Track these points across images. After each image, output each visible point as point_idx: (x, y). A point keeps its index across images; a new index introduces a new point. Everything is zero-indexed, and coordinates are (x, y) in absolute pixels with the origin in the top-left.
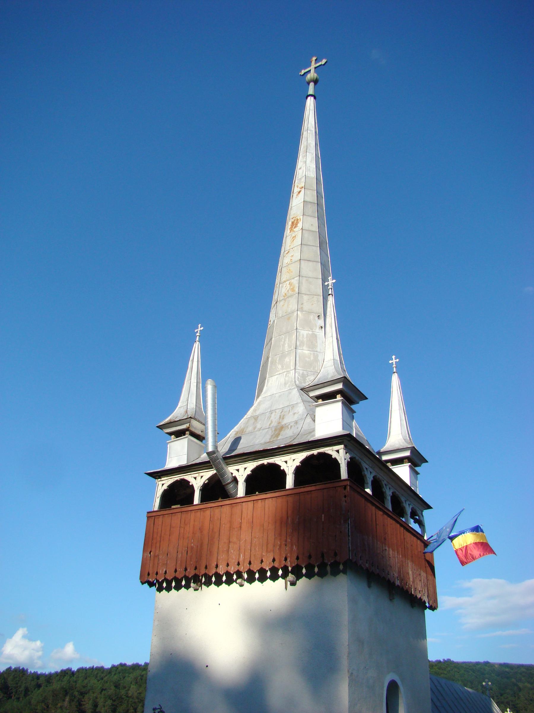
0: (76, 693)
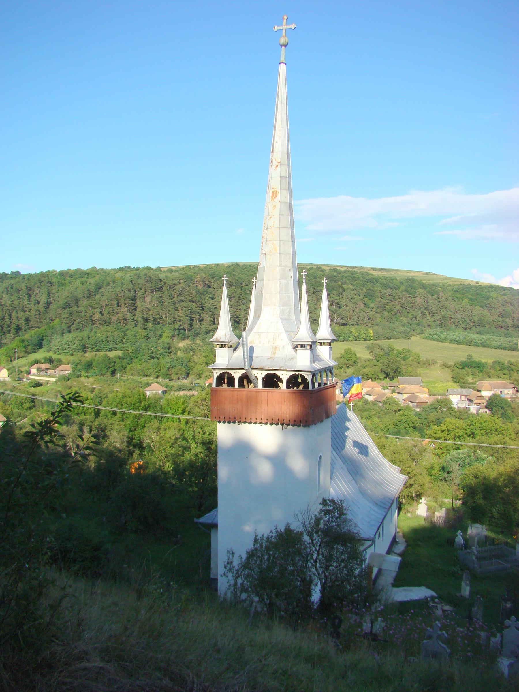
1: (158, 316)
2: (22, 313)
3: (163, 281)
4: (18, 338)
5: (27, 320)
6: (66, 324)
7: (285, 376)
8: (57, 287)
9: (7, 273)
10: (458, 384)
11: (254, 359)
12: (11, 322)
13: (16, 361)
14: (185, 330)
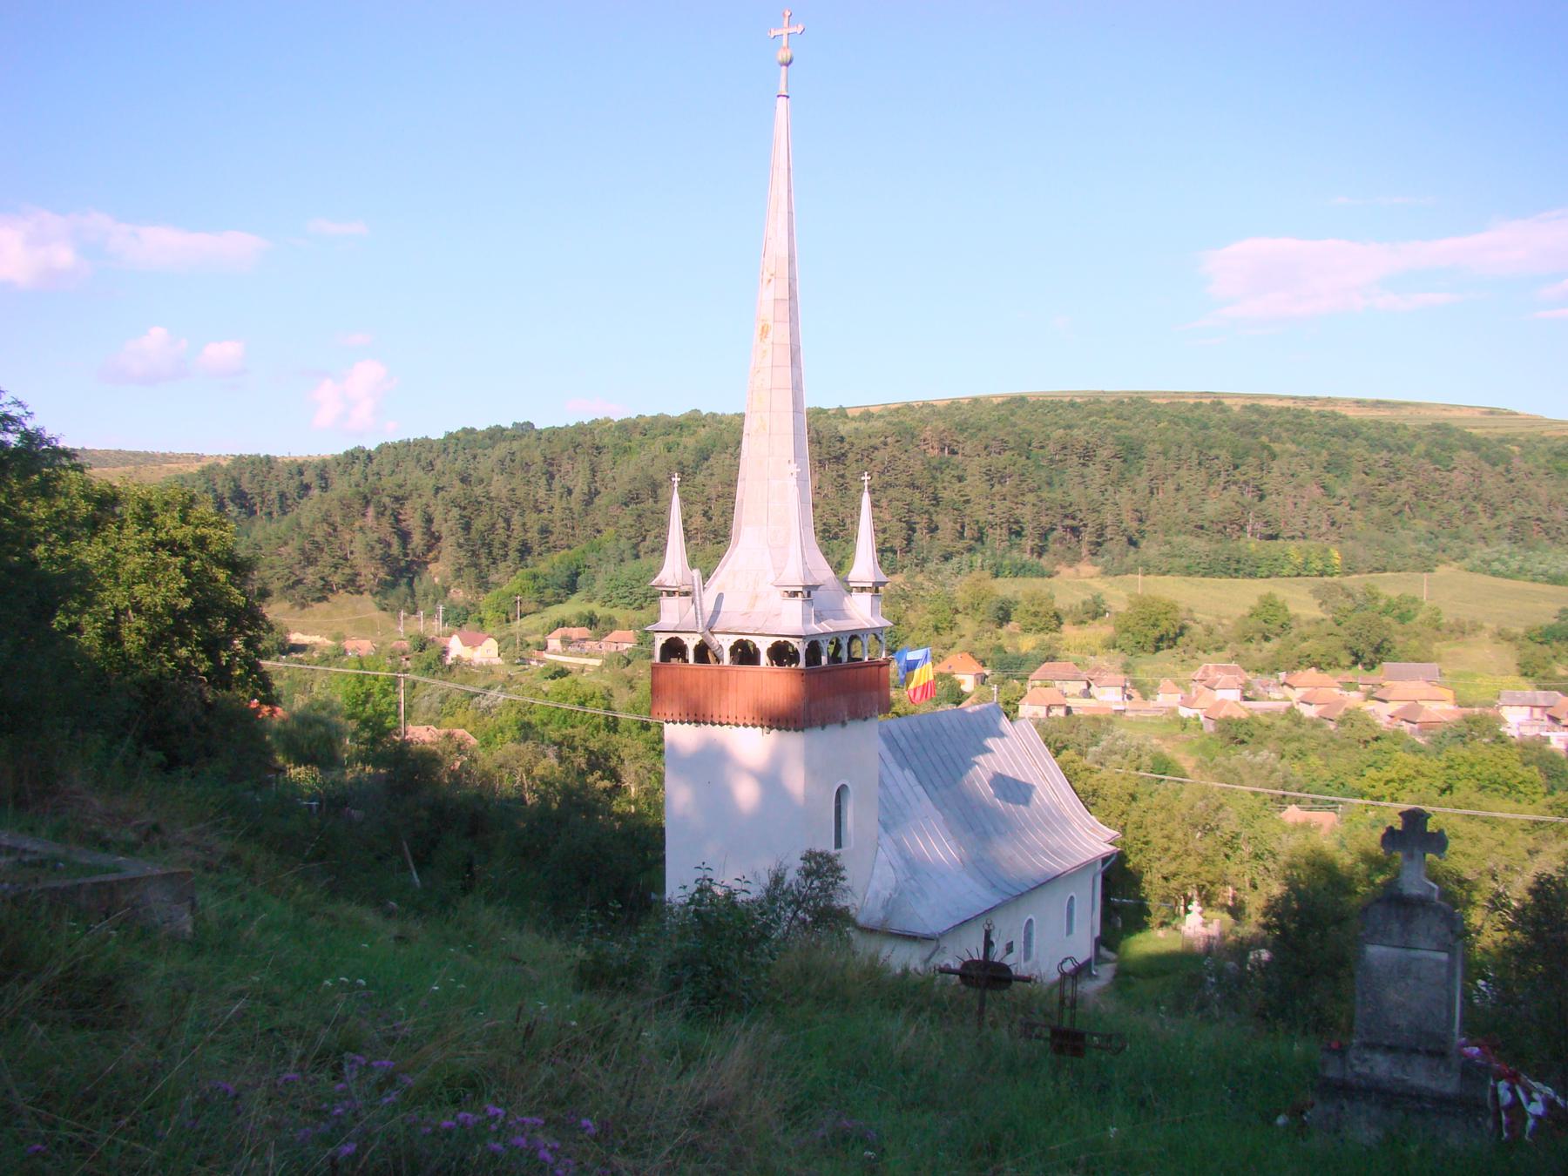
0: (387, 500)
1: (835, 519)
2: (534, 516)
3: (847, 440)
4: (526, 570)
5: (545, 531)
6: (629, 539)
7: (763, 645)
8: (610, 456)
9: (503, 425)
10: (1530, 680)
11: (720, 615)
12: (509, 537)
13: (519, 622)
14: (895, 552)
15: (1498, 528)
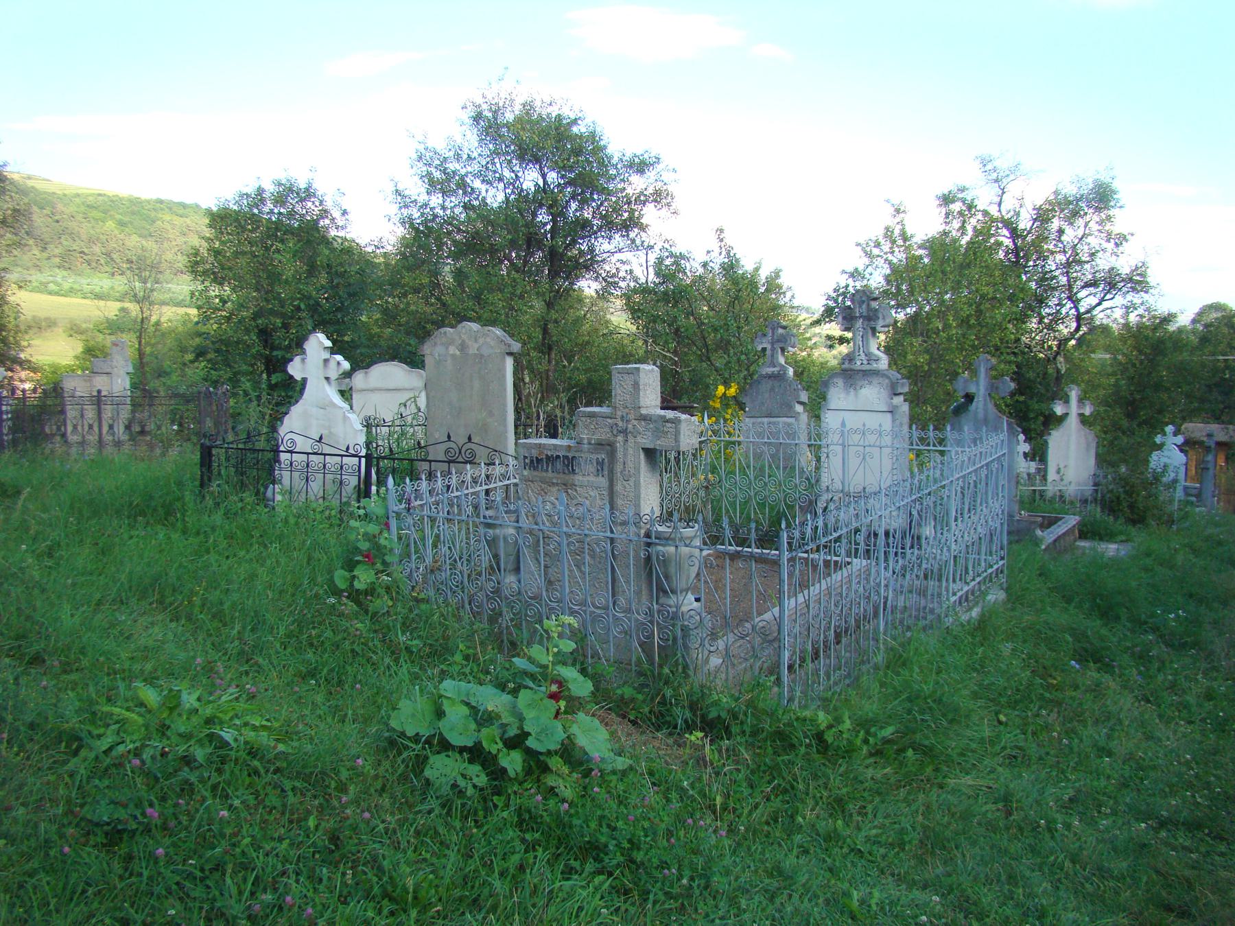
15: (49, 258)
